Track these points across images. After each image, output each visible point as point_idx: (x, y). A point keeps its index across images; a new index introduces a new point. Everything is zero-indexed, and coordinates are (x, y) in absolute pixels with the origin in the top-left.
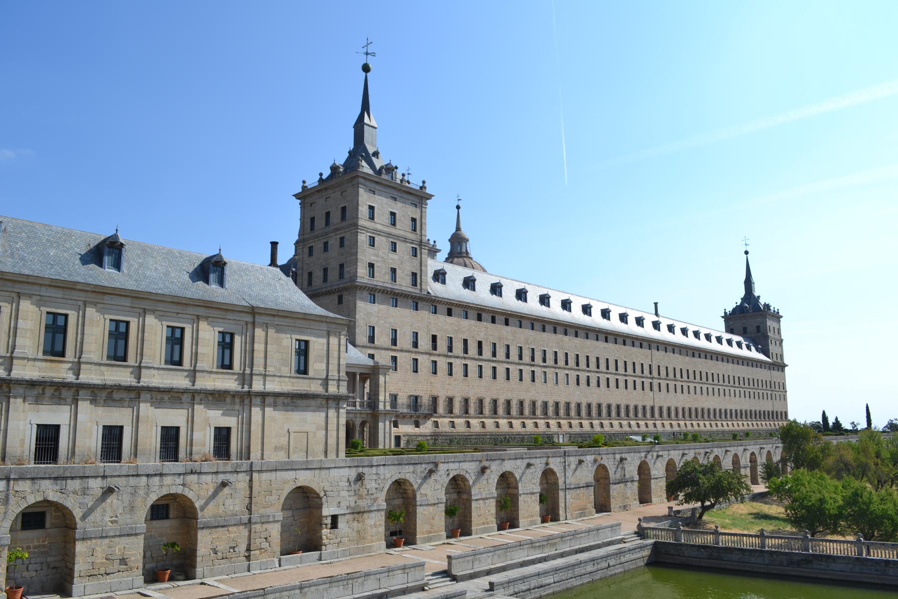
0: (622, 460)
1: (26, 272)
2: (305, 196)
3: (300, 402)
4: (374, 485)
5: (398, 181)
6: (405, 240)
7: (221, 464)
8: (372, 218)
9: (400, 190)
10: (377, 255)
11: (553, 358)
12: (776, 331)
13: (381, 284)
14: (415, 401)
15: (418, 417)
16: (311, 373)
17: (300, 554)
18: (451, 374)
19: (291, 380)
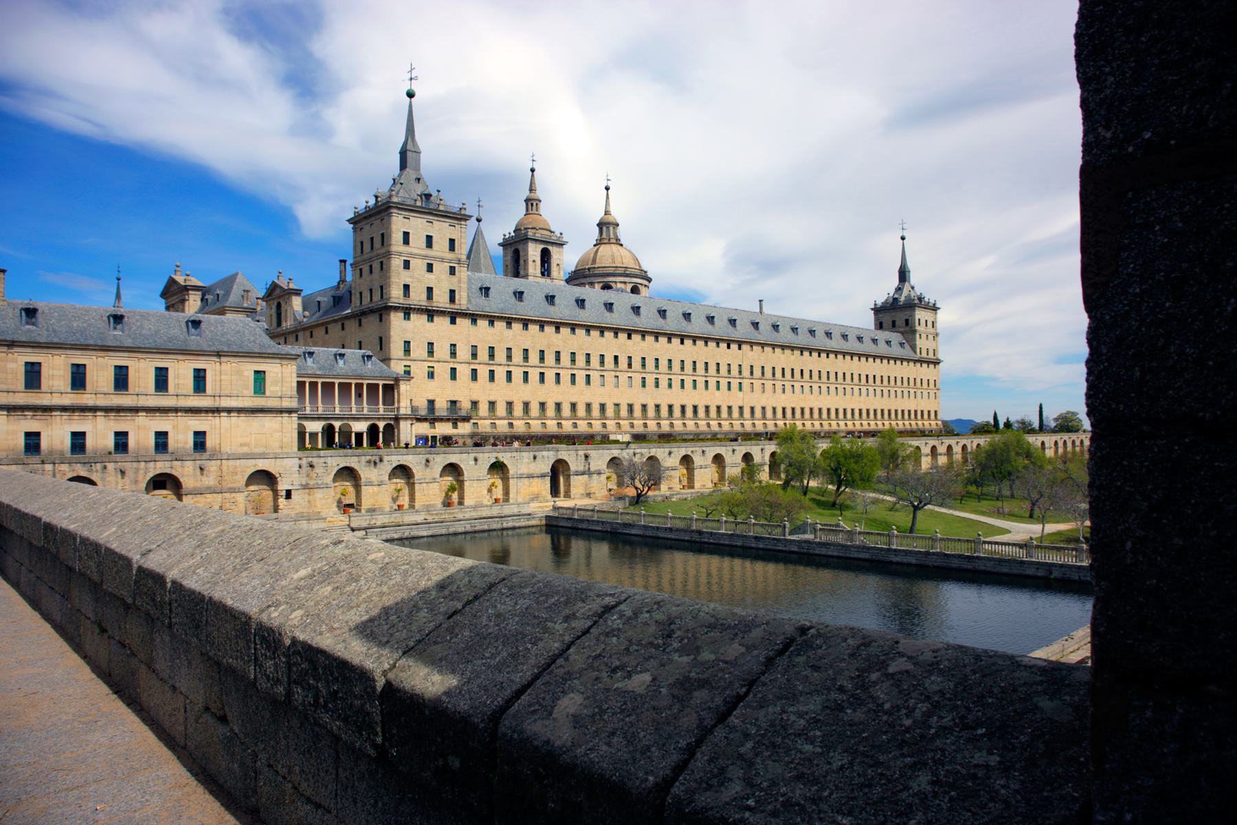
1: (56, 340)
6: (442, 260)
7: (197, 455)
12: (930, 324)
16: (268, 393)
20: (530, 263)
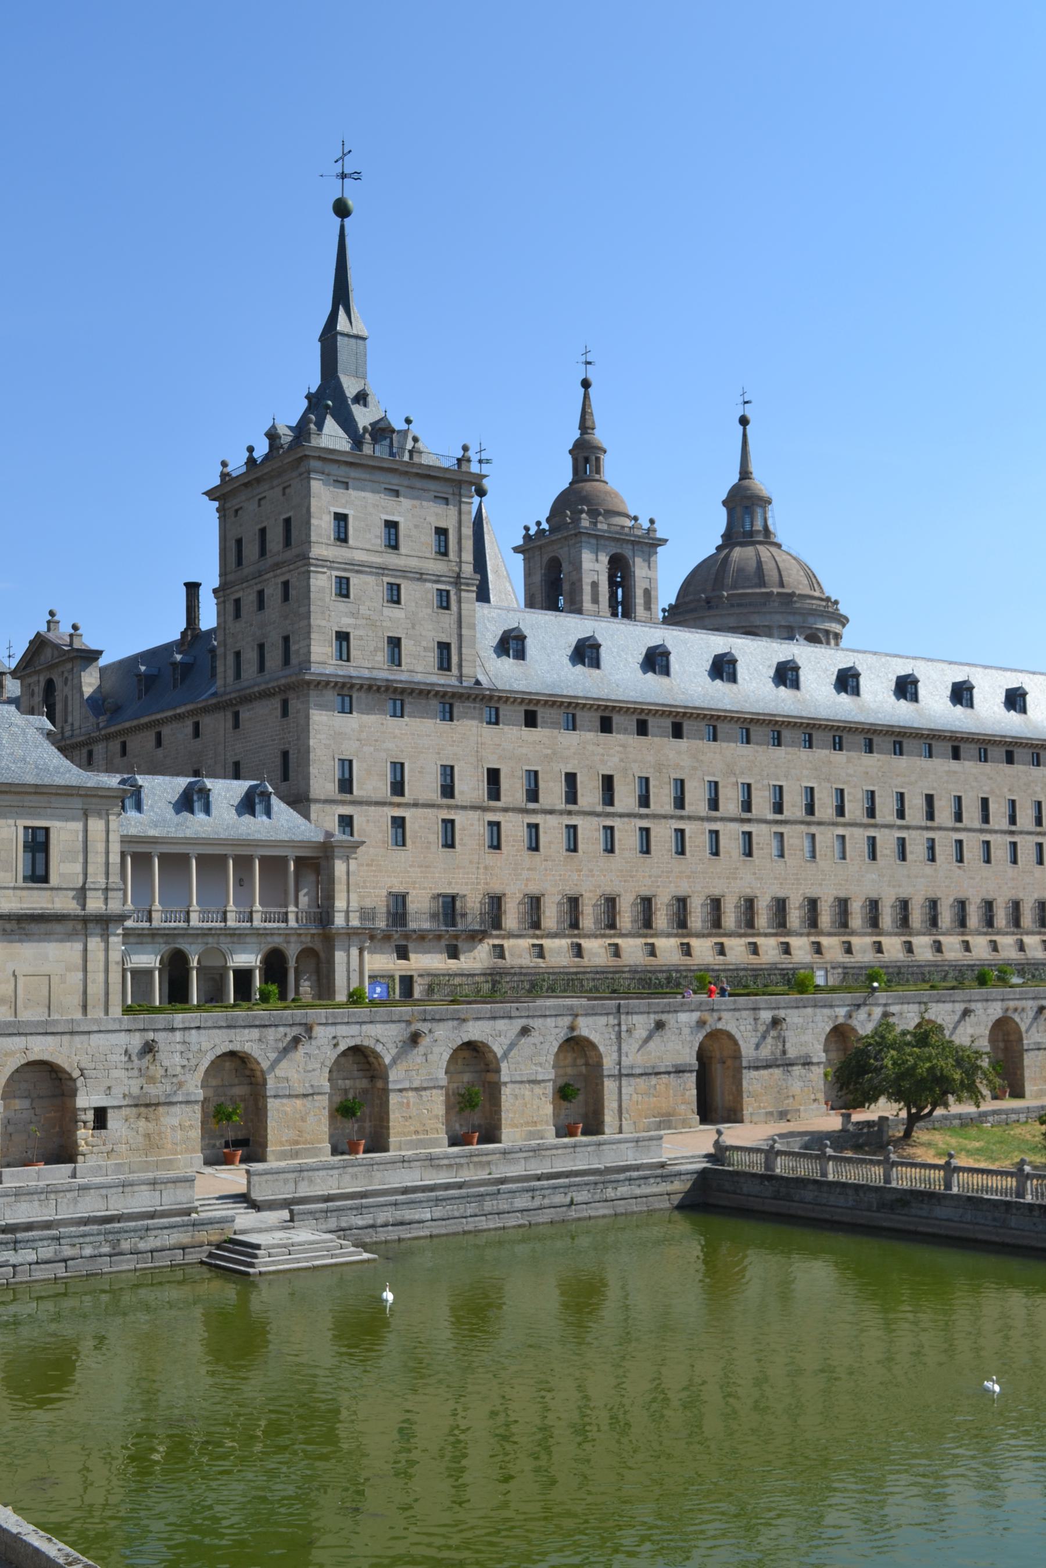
0: (776, 1022)
2: (227, 494)
3: (34, 927)
4: (177, 1059)
5: (406, 458)
6: (421, 577)
8: (342, 538)
9: (406, 473)
10: (354, 615)
11: (802, 801)
13: (366, 673)
14: (449, 907)
15: (456, 937)
16: (54, 880)
17: (42, 1167)
18: (535, 848)
19: (19, 892)
20: (587, 589)
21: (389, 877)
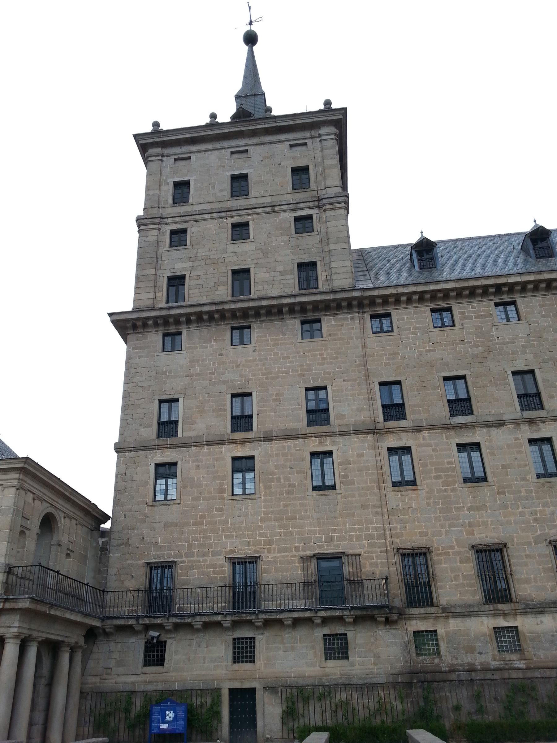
21: (227, 537)
